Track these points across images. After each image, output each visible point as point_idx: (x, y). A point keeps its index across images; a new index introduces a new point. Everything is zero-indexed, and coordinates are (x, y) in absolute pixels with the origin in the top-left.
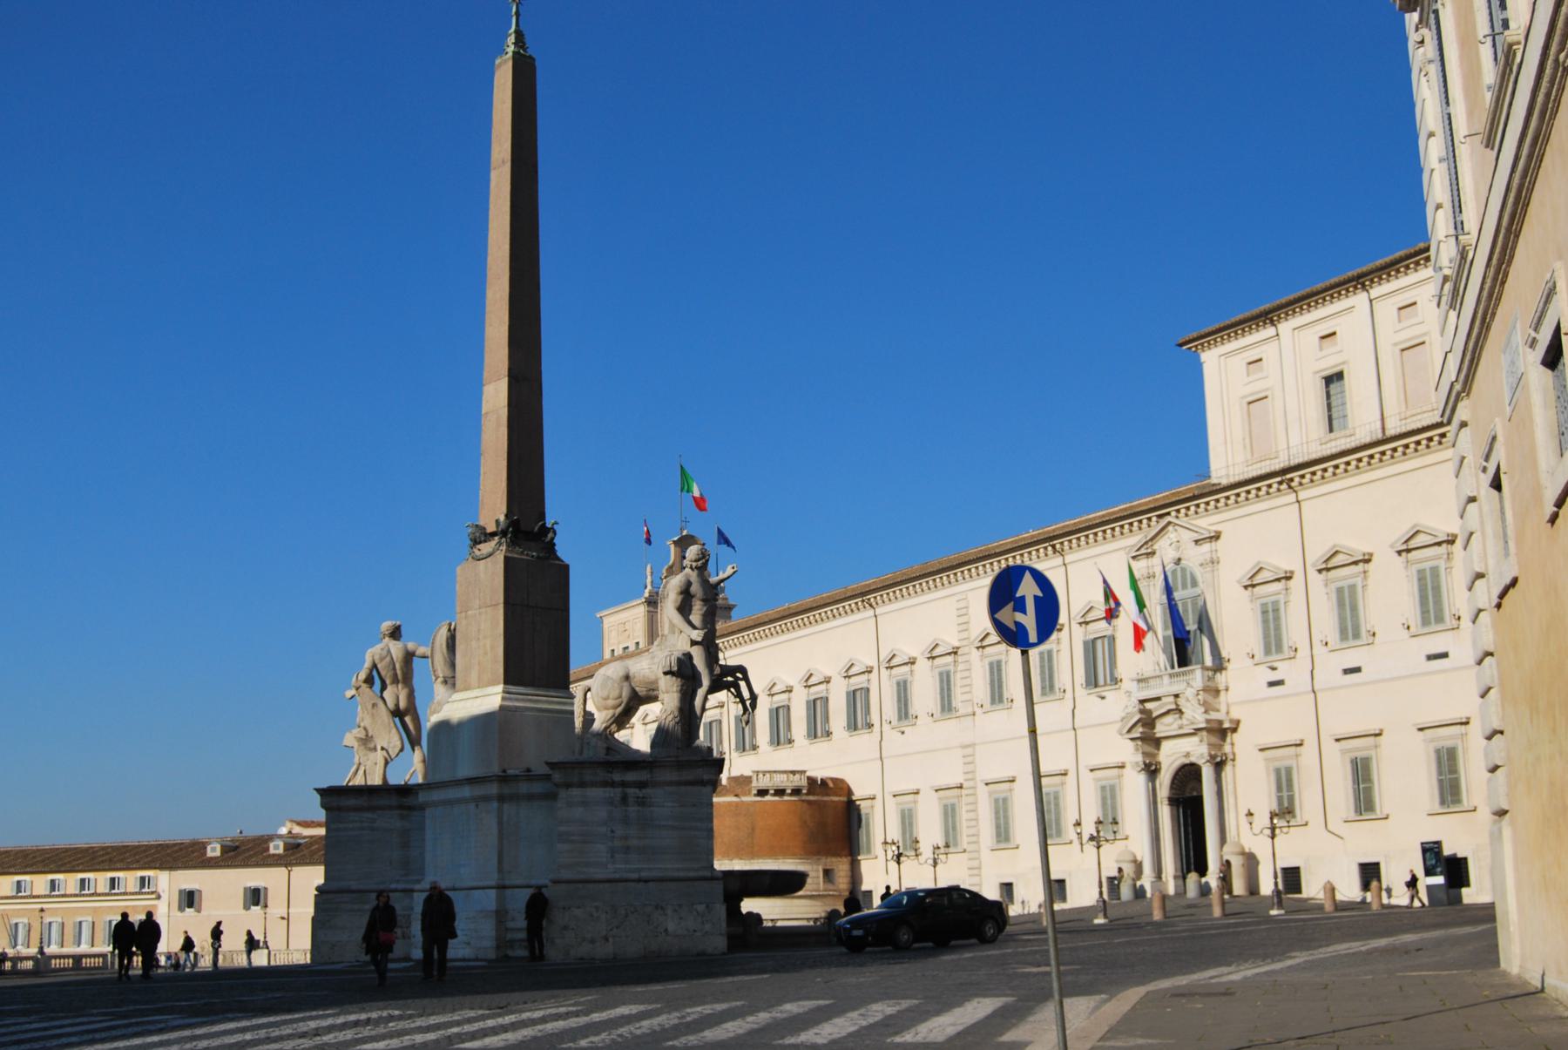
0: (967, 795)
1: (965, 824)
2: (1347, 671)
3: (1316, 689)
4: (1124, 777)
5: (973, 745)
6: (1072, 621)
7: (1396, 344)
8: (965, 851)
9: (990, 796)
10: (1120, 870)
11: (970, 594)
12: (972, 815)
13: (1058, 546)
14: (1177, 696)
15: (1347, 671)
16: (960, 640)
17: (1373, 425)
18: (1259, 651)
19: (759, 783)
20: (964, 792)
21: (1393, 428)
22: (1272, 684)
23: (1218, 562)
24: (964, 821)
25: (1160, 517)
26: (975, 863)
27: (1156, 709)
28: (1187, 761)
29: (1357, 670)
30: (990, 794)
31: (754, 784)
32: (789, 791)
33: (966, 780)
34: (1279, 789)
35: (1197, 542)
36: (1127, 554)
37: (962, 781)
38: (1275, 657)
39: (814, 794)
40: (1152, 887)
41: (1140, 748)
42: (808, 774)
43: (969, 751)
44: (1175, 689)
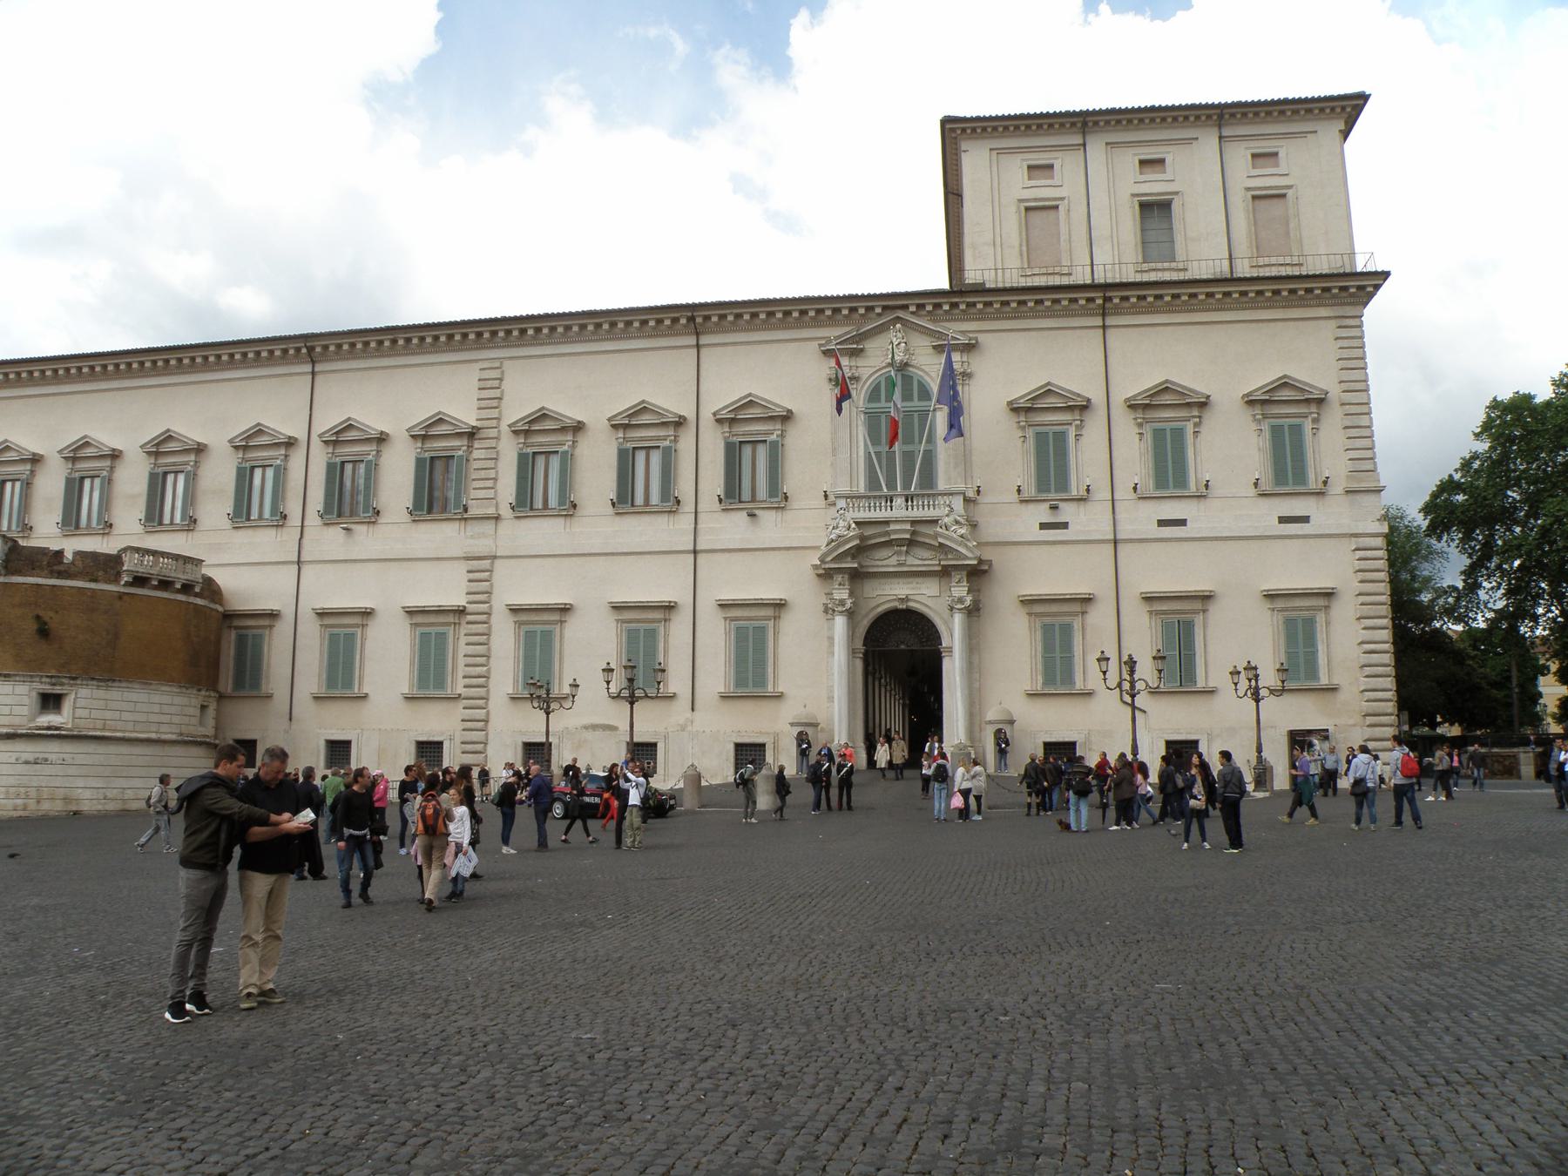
1: (461, 661)
2: (1162, 523)
4: (781, 620)
5: (495, 557)
7: (1248, 189)
11: (507, 363)
13: (699, 320)
15: (1162, 523)
16: (477, 420)
17: (1217, 262)
18: (1030, 491)
19: (130, 563)
20: (470, 618)
21: (1244, 269)
22: (1043, 526)
25: (885, 308)
29: (1182, 522)
32: (178, 586)
35: (934, 347)
36: (820, 345)
38: (1052, 495)
44: (917, 513)
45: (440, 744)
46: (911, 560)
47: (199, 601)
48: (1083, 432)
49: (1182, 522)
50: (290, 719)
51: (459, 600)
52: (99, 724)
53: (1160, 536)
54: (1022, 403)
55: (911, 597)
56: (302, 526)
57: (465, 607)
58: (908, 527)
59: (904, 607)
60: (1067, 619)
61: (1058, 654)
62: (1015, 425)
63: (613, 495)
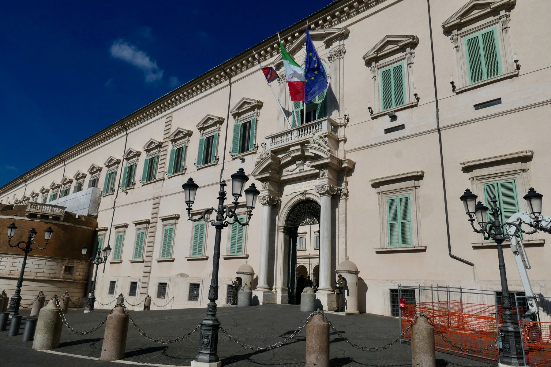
0: (151, 227)
1: (147, 244)
3: (440, 126)
5: (160, 197)
6: (230, 113)
8: (143, 262)
9: (163, 228)
10: (239, 279)
11: (174, 114)
12: (151, 239)
14: (304, 144)
16: (164, 139)
20: (151, 225)
22: (388, 131)
23: (345, 53)
24: (147, 243)
26: (147, 269)
27: (283, 158)
28: (302, 198)
29: (498, 101)
30: (164, 226)
31: (28, 209)
33: (152, 218)
34: (393, 215)
37: (150, 219)
39: (69, 222)
40: (264, 296)
41: (268, 187)
42: (66, 210)
43: (157, 201)
44: (303, 138)
45: (136, 283)
46: (306, 168)
47: (67, 224)
48: (414, 60)
49: (498, 101)
50: (104, 272)
51: (148, 217)
52: (8, 272)
53: (476, 117)
54: (372, 55)
55: (308, 192)
56: (117, 193)
57: (150, 220)
58: (299, 147)
59: (305, 198)
60: (404, 195)
61: (399, 221)
62: (370, 72)
63: (196, 161)
